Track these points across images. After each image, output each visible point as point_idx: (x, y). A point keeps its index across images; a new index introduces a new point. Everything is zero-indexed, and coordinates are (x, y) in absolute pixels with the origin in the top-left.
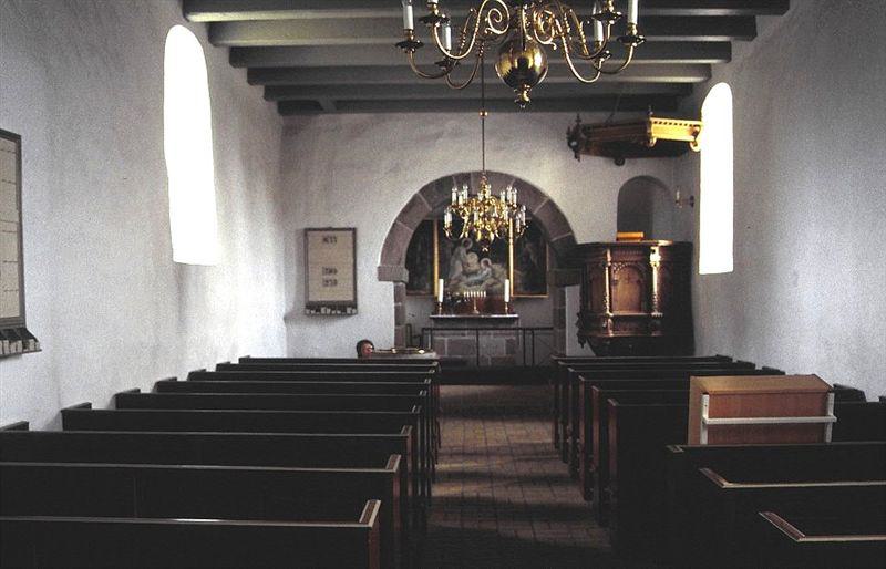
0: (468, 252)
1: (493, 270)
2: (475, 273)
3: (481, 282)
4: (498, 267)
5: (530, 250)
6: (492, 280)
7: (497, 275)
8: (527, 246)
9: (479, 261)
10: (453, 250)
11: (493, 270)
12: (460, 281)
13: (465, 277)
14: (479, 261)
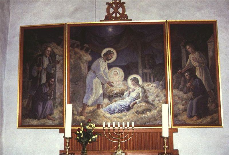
0: (110, 66)
1: (145, 91)
2: (120, 95)
3: (129, 108)
4: (151, 87)
5: (195, 64)
6: (144, 105)
7: (150, 99)
8: (191, 57)
9: (126, 79)
10: (90, 64)
11: (145, 91)
12: (99, 106)
13: (106, 101)
14: (126, 79)
